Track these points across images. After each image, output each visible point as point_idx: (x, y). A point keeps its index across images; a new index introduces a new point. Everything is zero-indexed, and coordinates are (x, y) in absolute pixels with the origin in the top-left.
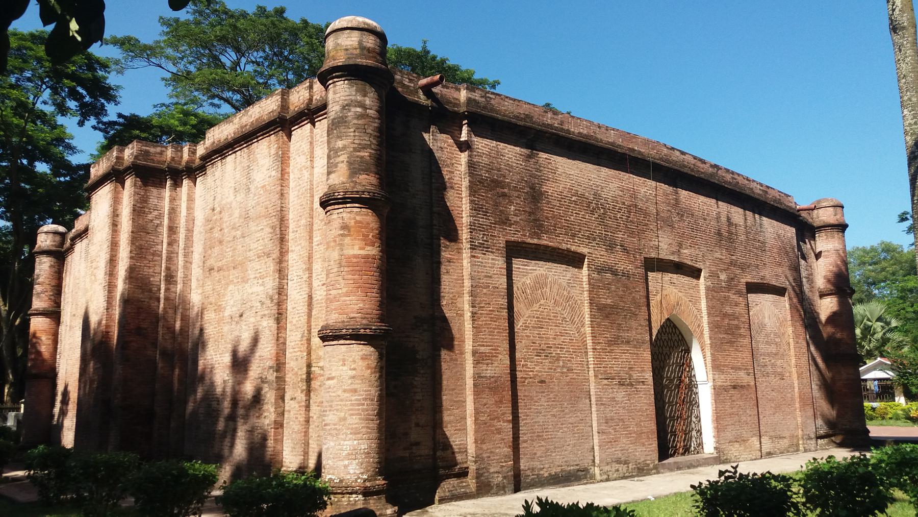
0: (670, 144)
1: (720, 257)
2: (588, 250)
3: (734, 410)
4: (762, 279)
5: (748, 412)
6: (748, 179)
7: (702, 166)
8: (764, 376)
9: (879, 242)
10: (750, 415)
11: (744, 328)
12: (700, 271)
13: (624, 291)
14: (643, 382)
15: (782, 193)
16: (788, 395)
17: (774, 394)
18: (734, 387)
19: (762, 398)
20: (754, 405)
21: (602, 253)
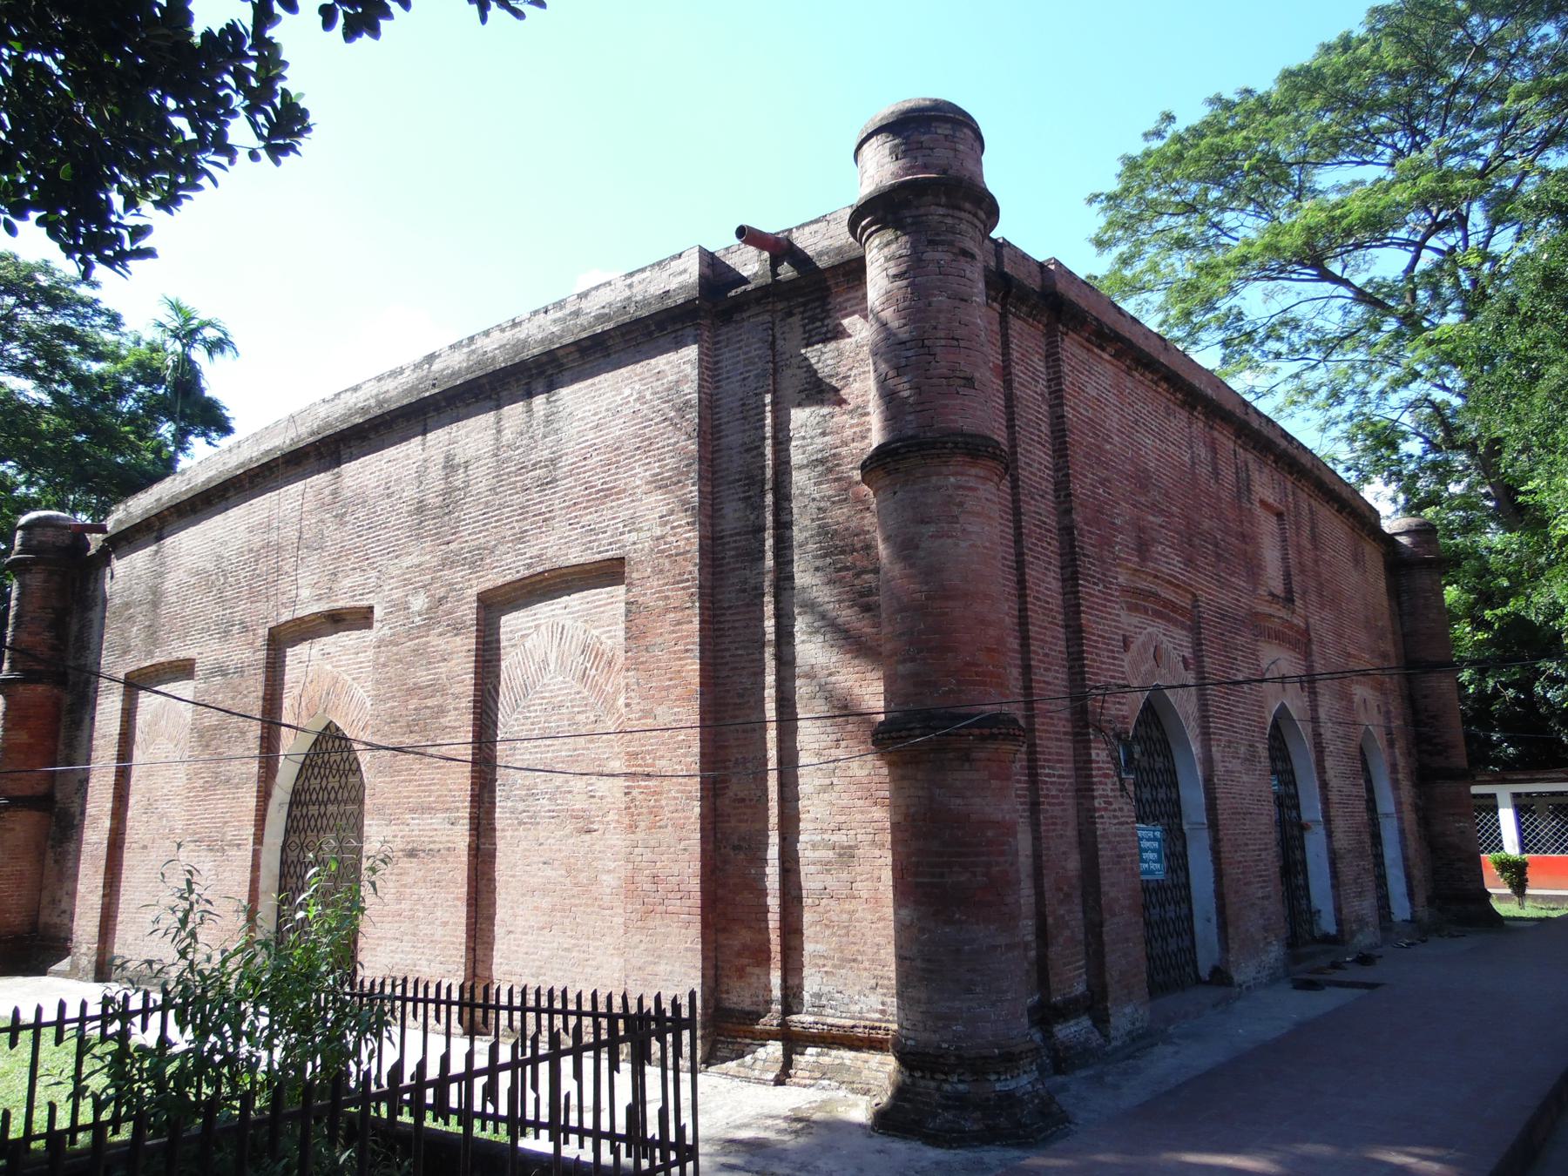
0: (328, 396)
1: (416, 561)
2: (198, 650)
3: (403, 906)
4: (529, 566)
5: (439, 914)
6: (515, 324)
7: (401, 379)
8: (521, 823)
9: (1332, 37)
10: (445, 924)
11: (455, 709)
12: (371, 609)
13: (233, 698)
14: (239, 845)
15: (643, 270)
16: (605, 877)
17: (549, 872)
18: (412, 854)
19: (507, 882)
20: (458, 899)
21: (215, 647)
